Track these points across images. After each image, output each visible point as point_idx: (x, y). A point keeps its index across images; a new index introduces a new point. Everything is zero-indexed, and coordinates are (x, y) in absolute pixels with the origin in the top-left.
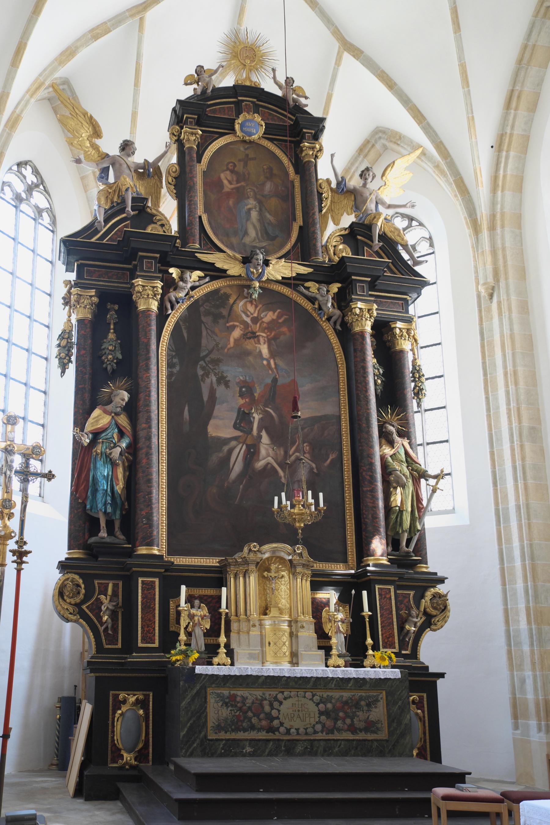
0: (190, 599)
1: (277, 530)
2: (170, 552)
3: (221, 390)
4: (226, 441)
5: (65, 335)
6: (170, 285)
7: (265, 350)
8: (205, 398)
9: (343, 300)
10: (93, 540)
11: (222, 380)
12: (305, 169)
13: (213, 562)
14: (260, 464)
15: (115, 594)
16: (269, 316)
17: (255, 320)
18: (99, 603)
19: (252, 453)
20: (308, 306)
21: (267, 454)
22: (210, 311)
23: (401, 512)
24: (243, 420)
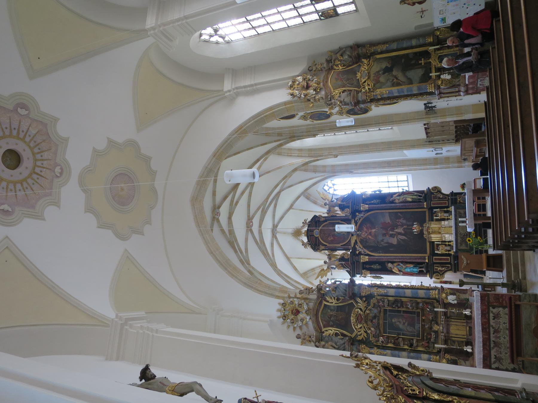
0: (438, 250)
1: (421, 233)
2: (426, 253)
3: (385, 241)
4: (398, 240)
5: (374, 277)
6: (360, 254)
7: (374, 230)
8: (387, 245)
9: (360, 212)
10: (425, 272)
11: (382, 241)
12: (326, 219)
13: (428, 244)
14: (403, 232)
15: (437, 266)
16: (365, 229)
17: (366, 232)
18: (440, 270)
19: (400, 234)
20: (361, 220)
21: (400, 230)
22: (364, 243)
23: (412, 199)
24: (392, 236)
